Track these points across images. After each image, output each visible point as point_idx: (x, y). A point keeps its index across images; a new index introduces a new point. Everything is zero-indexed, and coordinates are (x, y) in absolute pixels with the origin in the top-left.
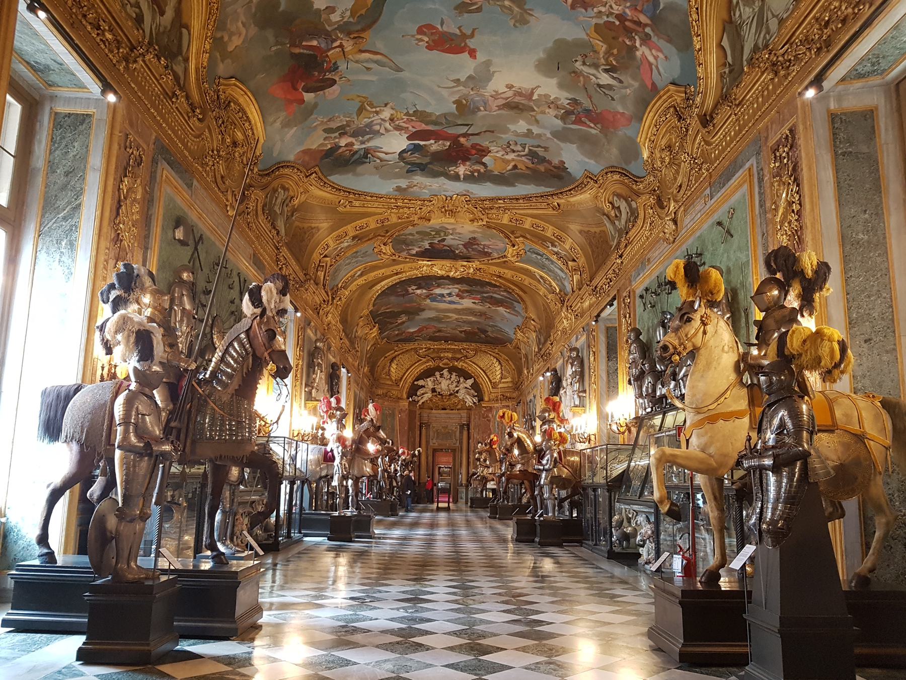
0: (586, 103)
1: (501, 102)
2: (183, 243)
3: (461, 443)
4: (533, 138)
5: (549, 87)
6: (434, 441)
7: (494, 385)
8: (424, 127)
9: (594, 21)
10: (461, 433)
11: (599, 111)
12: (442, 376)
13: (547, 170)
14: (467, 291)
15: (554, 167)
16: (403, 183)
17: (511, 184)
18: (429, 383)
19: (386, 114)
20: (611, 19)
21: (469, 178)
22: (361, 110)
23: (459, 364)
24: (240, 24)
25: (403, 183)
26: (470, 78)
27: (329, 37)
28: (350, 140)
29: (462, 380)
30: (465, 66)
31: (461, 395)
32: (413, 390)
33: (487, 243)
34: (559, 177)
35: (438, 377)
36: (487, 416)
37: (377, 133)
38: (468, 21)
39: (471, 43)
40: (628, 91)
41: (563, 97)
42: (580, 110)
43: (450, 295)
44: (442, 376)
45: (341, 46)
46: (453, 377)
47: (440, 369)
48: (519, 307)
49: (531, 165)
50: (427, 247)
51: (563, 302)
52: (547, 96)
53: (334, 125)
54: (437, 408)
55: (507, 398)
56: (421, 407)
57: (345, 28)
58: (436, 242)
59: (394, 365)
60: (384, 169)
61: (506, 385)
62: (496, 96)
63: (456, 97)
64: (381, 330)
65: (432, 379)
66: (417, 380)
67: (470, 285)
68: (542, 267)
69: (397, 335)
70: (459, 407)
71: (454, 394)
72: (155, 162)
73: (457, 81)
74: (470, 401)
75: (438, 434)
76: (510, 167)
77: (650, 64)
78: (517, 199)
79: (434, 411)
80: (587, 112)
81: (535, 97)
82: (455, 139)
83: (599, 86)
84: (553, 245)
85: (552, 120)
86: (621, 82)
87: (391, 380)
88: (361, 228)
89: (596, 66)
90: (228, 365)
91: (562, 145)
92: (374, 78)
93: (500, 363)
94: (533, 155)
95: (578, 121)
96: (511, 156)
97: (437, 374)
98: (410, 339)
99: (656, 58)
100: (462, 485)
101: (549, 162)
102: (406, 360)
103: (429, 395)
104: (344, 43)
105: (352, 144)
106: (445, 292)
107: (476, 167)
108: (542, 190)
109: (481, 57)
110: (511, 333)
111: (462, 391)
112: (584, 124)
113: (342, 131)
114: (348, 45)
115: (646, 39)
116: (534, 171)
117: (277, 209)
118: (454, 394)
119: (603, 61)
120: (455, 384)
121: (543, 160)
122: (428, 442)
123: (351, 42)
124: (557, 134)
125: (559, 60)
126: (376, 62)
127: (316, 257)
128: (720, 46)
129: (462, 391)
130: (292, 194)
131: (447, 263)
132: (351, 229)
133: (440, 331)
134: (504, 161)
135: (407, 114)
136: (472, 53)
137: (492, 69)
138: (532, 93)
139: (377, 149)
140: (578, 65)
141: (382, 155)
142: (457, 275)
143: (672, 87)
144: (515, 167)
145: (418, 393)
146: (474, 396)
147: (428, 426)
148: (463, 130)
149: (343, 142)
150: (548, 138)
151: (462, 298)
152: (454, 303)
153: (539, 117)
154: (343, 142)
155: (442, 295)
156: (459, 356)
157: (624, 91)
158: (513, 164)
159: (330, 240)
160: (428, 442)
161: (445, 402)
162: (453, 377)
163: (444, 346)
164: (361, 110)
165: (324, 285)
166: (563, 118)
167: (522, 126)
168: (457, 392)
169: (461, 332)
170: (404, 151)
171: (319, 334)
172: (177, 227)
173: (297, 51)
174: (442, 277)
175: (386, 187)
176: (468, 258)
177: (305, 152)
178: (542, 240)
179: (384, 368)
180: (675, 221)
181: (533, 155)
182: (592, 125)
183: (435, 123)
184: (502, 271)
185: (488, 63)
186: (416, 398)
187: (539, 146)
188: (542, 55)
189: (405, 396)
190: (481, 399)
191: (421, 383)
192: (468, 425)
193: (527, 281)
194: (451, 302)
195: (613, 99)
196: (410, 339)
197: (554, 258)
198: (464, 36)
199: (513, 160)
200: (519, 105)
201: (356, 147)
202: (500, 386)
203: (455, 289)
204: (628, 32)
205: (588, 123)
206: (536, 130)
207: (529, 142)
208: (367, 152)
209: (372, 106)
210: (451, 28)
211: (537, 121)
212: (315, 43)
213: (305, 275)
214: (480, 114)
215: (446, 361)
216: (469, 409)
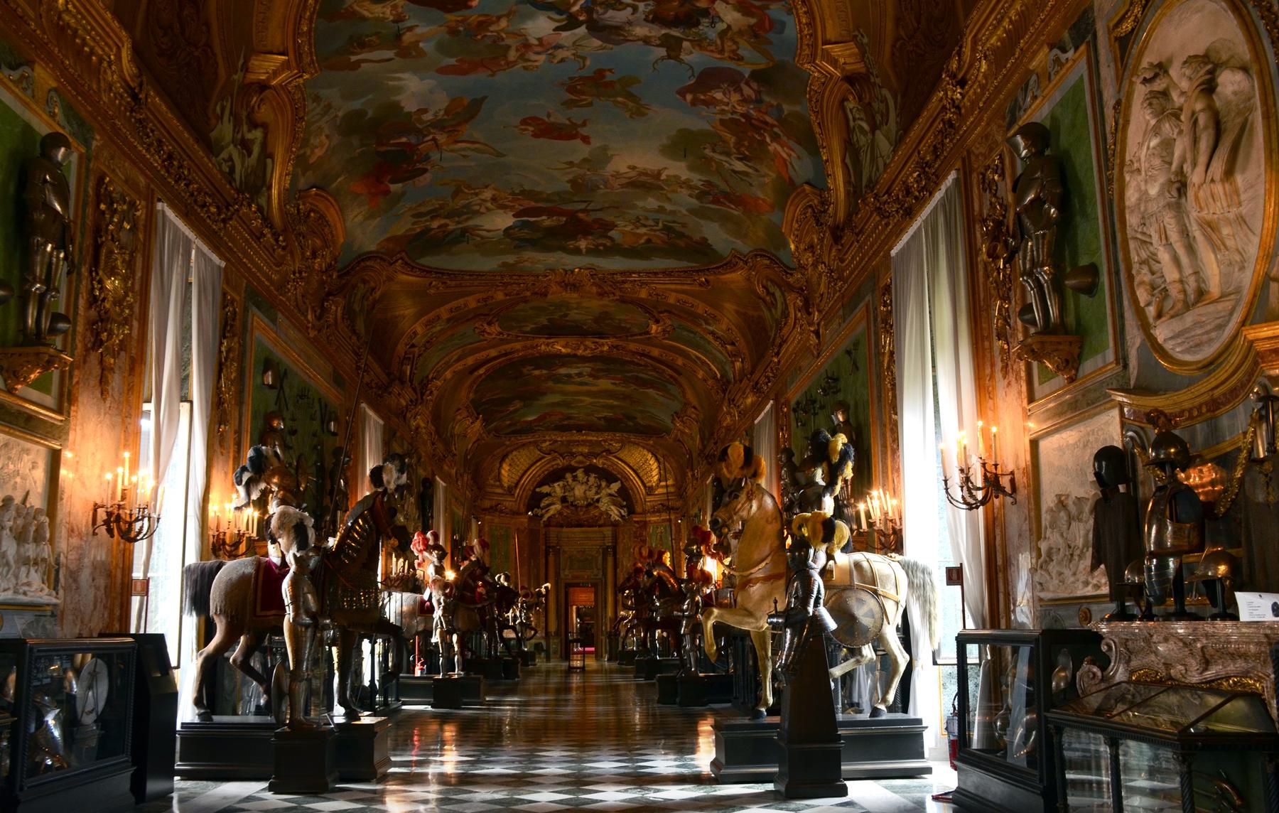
0: (723, 186)
1: (624, 181)
2: (271, 387)
3: (605, 574)
5: (678, 169)
6: (567, 572)
7: (650, 490)
8: (533, 204)
9: (718, 117)
10: (605, 559)
12: (575, 478)
14: (602, 370)
16: (511, 259)
17: (648, 258)
18: (558, 488)
19: (487, 194)
20: (735, 116)
21: (592, 252)
22: (456, 193)
23: (598, 462)
24: (323, 137)
25: (511, 259)
26: (585, 160)
27: (420, 133)
28: (443, 221)
29: (604, 484)
30: (579, 151)
32: (535, 500)
33: (623, 317)
35: (570, 480)
36: (641, 535)
37: (477, 213)
38: (577, 114)
39: (584, 131)
40: (767, 180)
41: (697, 179)
43: (580, 375)
44: (575, 478)
45: (434, 139)
46: (592, 479)
47: (573, 470)
48: (674, 390)
50: (545, 322)
51: (724, 391)
52: (675, 176)
53: (423, 209)
54: (570, 525)
55: (668, 509)
56: (548, 524)
57: (438, 125)
58: (556, 317)
59: (506, 467)
60: (486, 246)
62: (617, 175)
63: (570, 177)
64: (486, 421)
66: (541, 484)
67: (605, 364)
68: (697, 347)
69: (510, 425)
70: (601, 522)
71: (593, 504)
72: (246, 310)
73: (571, 164)
74: (615, 513)
76: (642, 241)
77: (785, 160)
78: (656, 274)
79: (565, 529)
80: (726, 196)
81: (663, 177)
82: (572, 215)
83: (734, 171)
84: (707, 323)
85: (685, 199)
86: (757, 170)
87: (502, 486)
88: (458, 308)
89: (728, 154)
90: (354, 539)
91: (702, 222)
92: (472, 164)
93: (657, 459)
94: (668, 229)
95: (716, 201)
96: (642, 230)
97: (568, 475)
98: (528, 429)
99: (789, 156)
101: (691, 238)
102: (522, 458)
103: (558, 506)
104: (438, 137)
105: (447, 225)
106: (574, 371)
107: (600, 241)
108: (684, 264)
109: (596, 143)
110: (668, 421)
111: (605, 500)
113: (434, 214)
114: (442, 138)
115: (775, 138)
117: (356, 307)
118: (593, 504)
120: (594, 490)
121: (682, 235)
122: (557, 574)
123: (445, 135)
124: (692, 211)
125: (683, 145)
126: (475, 150)
127: (401, 348)
128: (843, 161)
129: (605, 500)
130: (372, 284)
131: (572, 341)
132: (444, 312)
133: (569, 418)
134: (635, 234)
135: (513, 194)
136: (586, 140)
137: (610, 153)
138: (659, 174)
139: (477, 228)
140: (708, 152)
141: (484, 233)
142: (588, 353)
143: (807, 187)
144: (649, 241)
146: (622, 507)
147: (557, 553)
148: (583, 206)
149: (435, 224)
151: (597, 378)
152: (586, 384)
154: (435, 224)
155: (569, 376)
156: (598, 450)
159: (419, 329)
160: (557, 574)
161: (580, 516)
162: (592, 479)
163: (577, 437)
164: (456, 193)
165: (411, 381)
166: (698, 197)
167: (652, 202)
168: (598, 501)
169: (599, 419)
170: (510, 228)
171: (406, 445)
172: (265, 372)
173: (383, 149)
174: (568, 355)
175: (489, 264)
176: (601, 335)
177: (388, 240)
178: (693, 317)
180: (817, 333)
183: (548, 201)
184: (647, 349)
185: (605, 149)
186: (539, 512)
188: (665, 141)
190: (631, 511)
191: (545, 489)
192: (614, 548)
193: (680, 361)
194: (581, 384)
196: (528, 429)
197: (710, 338)
198: (574, 126)
200: (646, 183)
201: (451, 227)
203: (586, 369)
204: (756, 129)
206: (668, 207)
208: (465, 231)
209: (469, 187)
210: (560, 118)
211: (669, 200)
212: (404, 140)
213: (388, 375)
214: (600, 192)
215: (580, 458)
216: (615, 525)
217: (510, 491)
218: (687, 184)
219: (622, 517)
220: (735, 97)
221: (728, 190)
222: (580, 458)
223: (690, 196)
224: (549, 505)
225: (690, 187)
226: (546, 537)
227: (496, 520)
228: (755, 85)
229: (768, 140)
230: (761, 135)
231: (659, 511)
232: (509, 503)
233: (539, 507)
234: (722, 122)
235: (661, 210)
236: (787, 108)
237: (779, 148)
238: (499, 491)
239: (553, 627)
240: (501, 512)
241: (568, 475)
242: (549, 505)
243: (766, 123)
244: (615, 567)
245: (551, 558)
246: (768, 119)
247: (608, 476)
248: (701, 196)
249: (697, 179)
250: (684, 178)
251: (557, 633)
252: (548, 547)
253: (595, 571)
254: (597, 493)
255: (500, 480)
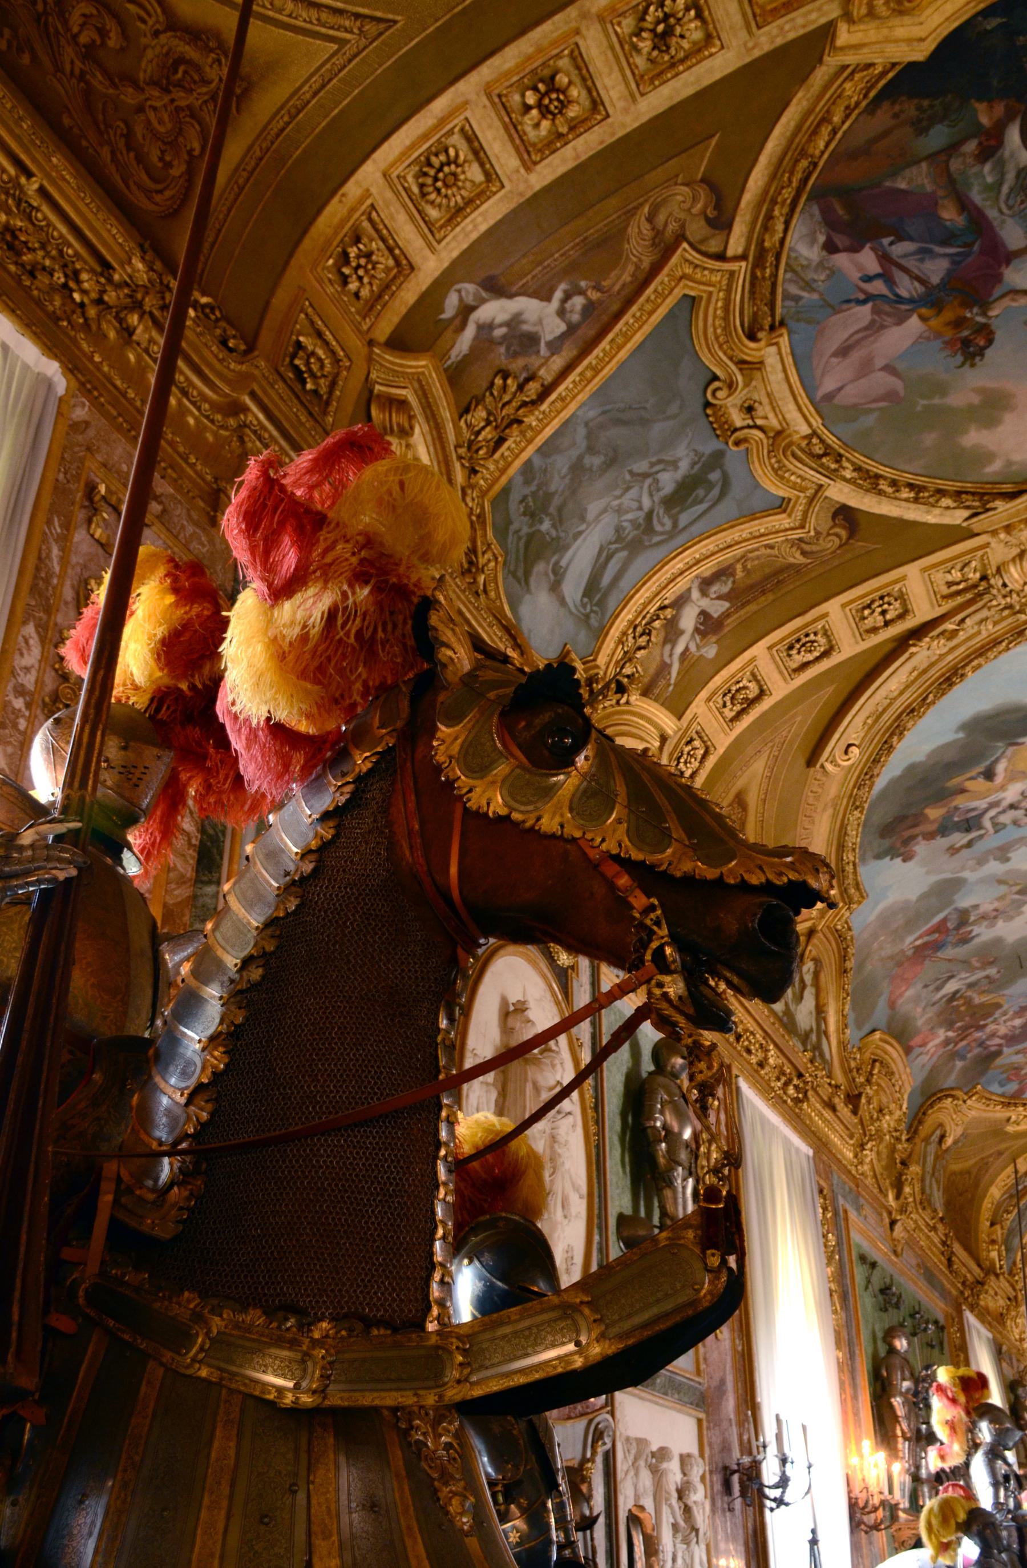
0: (949, 952)
4: (989, 852)
9: (1005, 1007)
11: (927, 962)
13: (919, 818)
15: (913, 838)
34: (886, 830)
40: (919, 1010)
41: (983, 933)
42: (950, 939)
49: (961, 802)
52: (1010, 918)
76: (1001, 768)
80: (937, 946)
86: (934, 1004)
89: (970, 986)
91: (934, 878)
94: (971, 824)
95: (941, 928)
101: (930, 836)
112: (930, 932)
115: (947, 1042)
116: (942, 796)
119: (969, 993)
121: (944, 829)
124: (955, 885)
140: (992, 971)
144: (989, 775)
150: (963, 868)
153: (1003, 889)
157: (923, 1004)
158: (999, 779)
181: (971, 824)
182: (919, 942)
187: (969, 845)
195: (926, 986)
199: (1003, 788)
204: (964, 1029)
205: (926, 939)
206: (993, 867)
207: (992, 841)
211: (1001, 882)
218: (990, 918)
220: (1003, 1030)
221: (939, 954)
223: (976, 907)
225: (984, 917)
228: (993, 1049)
229: (950, 1034)
230: (959, 1028)
234: (998, 1006)
235: (1002, 854)
236: (959, 1064)
237: (937, 1041)
243: (962, 1040)
246: (964, 1043)
248: (963, 917)
249: (983, 933)
250: (1000, 923)
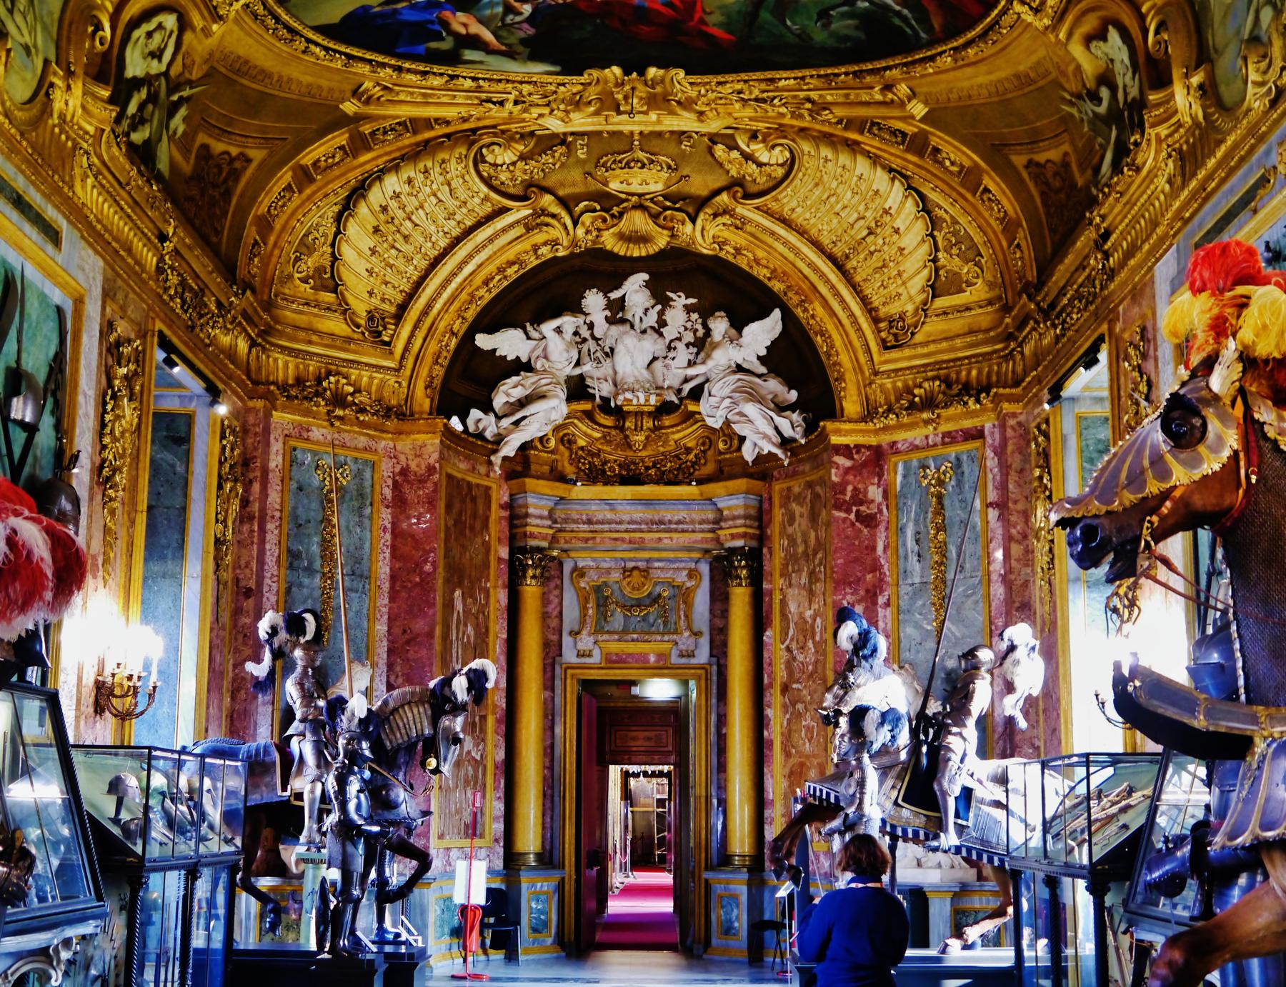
3: (720, 649)
6: (586, 642)
7: (895, 333)
10: (720, 600)
18: (554, 345)
23: (703, 235)
29: (720, 326)
31: (713, 411)
32: (471, 379)
46: (677, 317)
47: (604, 270)
54: (595, 475)
56: (520, 466)
59: (358, 233)
61: (957, 324)
65: (568, 322)
66: (492, 319)
70: (709, 469)
71: (678, 406)
74: (761, 431)
75: (603, 604)
79: (581, 491)
87: (345, 311)
93: (926, 207)
97: (594, 301)
100: (725, 859)
111: (721, 389)
120: (683, 354)
122: (551, 651)
145: (499, 401)
146: (781, 408)
147: (551, 571)
156: (699, 184)
160: (551, 651)
161: (635, 443)
162: (677, 317)
168: (696, 394)
179: (306, 247)
189: (422, 401)
191: (509, 343)
192: (755, 558)
202: (933, 327)
215: (638, 221)
216: (763, 469)
217: (376, 329)
219: (785, 442)
222: (638, 221)
224: (522, 403)
226: (516, 516)
227: (319, 433)
231: (929, 403)
232: (372, 374)
233: (487, 408)
238: (336, 325)
239: (530, 840)
240: (339, 400)
241: (594, 301)
242: (522, 403)
244: (759, 623)
245: (531, 590)
247: (731, 293)
251: (548, 859)
252: (518, 549)
253: (685, 640)
254: (691, 364)
255: (334, 285)
